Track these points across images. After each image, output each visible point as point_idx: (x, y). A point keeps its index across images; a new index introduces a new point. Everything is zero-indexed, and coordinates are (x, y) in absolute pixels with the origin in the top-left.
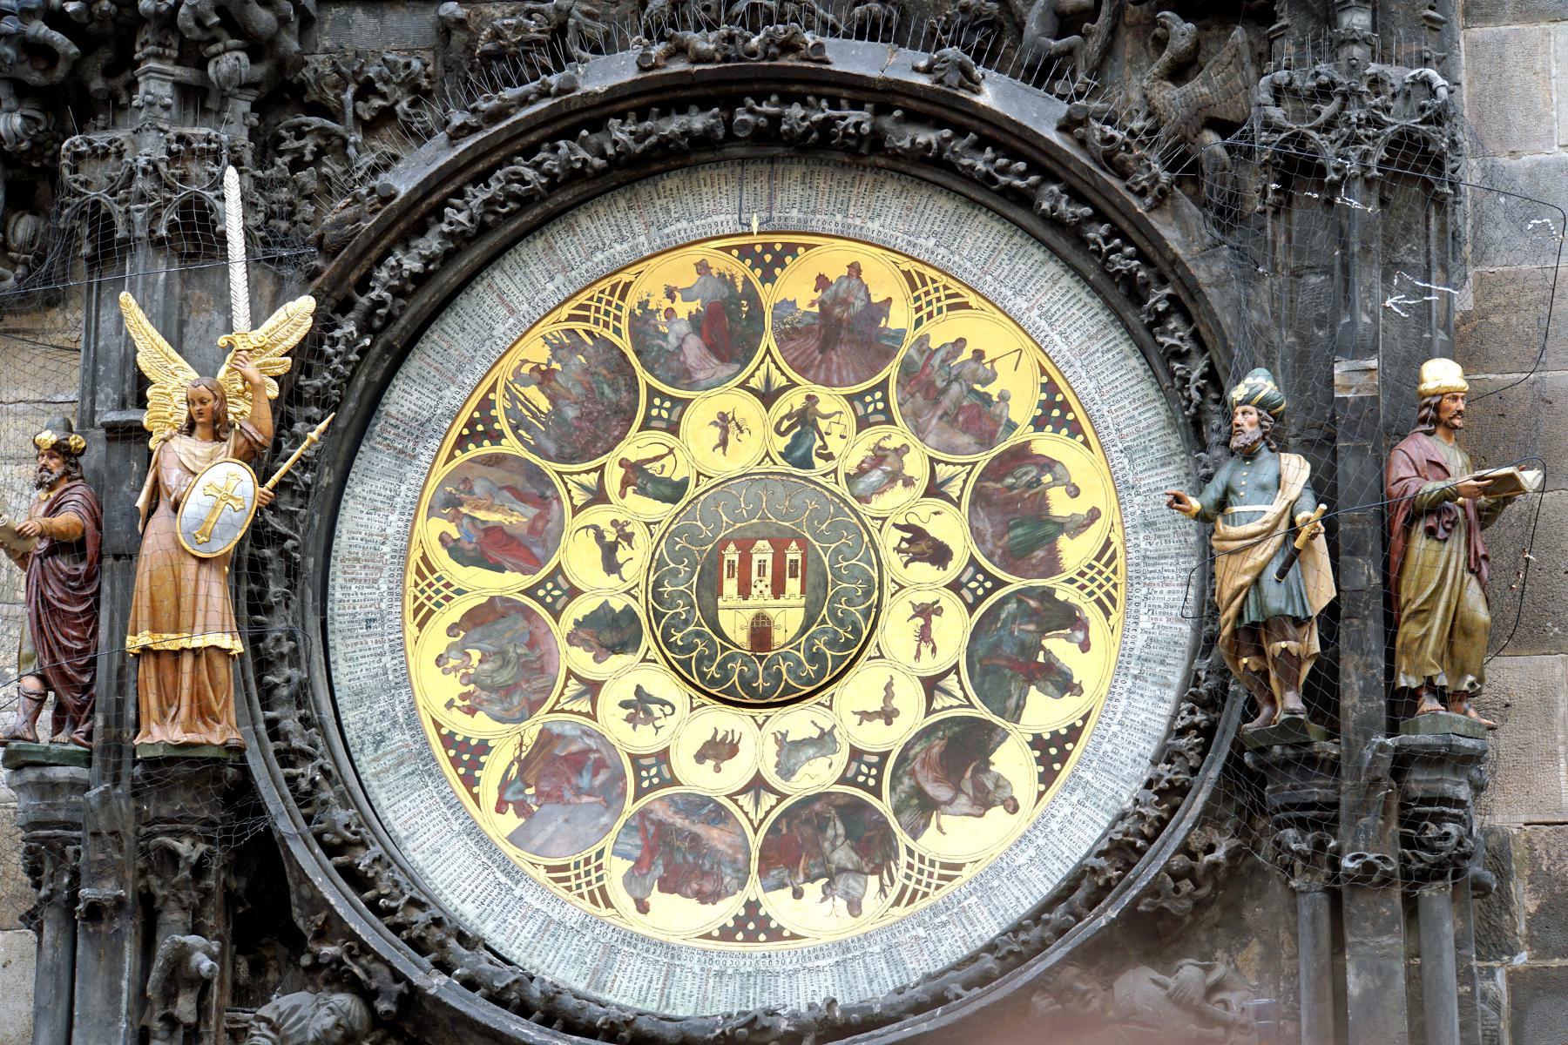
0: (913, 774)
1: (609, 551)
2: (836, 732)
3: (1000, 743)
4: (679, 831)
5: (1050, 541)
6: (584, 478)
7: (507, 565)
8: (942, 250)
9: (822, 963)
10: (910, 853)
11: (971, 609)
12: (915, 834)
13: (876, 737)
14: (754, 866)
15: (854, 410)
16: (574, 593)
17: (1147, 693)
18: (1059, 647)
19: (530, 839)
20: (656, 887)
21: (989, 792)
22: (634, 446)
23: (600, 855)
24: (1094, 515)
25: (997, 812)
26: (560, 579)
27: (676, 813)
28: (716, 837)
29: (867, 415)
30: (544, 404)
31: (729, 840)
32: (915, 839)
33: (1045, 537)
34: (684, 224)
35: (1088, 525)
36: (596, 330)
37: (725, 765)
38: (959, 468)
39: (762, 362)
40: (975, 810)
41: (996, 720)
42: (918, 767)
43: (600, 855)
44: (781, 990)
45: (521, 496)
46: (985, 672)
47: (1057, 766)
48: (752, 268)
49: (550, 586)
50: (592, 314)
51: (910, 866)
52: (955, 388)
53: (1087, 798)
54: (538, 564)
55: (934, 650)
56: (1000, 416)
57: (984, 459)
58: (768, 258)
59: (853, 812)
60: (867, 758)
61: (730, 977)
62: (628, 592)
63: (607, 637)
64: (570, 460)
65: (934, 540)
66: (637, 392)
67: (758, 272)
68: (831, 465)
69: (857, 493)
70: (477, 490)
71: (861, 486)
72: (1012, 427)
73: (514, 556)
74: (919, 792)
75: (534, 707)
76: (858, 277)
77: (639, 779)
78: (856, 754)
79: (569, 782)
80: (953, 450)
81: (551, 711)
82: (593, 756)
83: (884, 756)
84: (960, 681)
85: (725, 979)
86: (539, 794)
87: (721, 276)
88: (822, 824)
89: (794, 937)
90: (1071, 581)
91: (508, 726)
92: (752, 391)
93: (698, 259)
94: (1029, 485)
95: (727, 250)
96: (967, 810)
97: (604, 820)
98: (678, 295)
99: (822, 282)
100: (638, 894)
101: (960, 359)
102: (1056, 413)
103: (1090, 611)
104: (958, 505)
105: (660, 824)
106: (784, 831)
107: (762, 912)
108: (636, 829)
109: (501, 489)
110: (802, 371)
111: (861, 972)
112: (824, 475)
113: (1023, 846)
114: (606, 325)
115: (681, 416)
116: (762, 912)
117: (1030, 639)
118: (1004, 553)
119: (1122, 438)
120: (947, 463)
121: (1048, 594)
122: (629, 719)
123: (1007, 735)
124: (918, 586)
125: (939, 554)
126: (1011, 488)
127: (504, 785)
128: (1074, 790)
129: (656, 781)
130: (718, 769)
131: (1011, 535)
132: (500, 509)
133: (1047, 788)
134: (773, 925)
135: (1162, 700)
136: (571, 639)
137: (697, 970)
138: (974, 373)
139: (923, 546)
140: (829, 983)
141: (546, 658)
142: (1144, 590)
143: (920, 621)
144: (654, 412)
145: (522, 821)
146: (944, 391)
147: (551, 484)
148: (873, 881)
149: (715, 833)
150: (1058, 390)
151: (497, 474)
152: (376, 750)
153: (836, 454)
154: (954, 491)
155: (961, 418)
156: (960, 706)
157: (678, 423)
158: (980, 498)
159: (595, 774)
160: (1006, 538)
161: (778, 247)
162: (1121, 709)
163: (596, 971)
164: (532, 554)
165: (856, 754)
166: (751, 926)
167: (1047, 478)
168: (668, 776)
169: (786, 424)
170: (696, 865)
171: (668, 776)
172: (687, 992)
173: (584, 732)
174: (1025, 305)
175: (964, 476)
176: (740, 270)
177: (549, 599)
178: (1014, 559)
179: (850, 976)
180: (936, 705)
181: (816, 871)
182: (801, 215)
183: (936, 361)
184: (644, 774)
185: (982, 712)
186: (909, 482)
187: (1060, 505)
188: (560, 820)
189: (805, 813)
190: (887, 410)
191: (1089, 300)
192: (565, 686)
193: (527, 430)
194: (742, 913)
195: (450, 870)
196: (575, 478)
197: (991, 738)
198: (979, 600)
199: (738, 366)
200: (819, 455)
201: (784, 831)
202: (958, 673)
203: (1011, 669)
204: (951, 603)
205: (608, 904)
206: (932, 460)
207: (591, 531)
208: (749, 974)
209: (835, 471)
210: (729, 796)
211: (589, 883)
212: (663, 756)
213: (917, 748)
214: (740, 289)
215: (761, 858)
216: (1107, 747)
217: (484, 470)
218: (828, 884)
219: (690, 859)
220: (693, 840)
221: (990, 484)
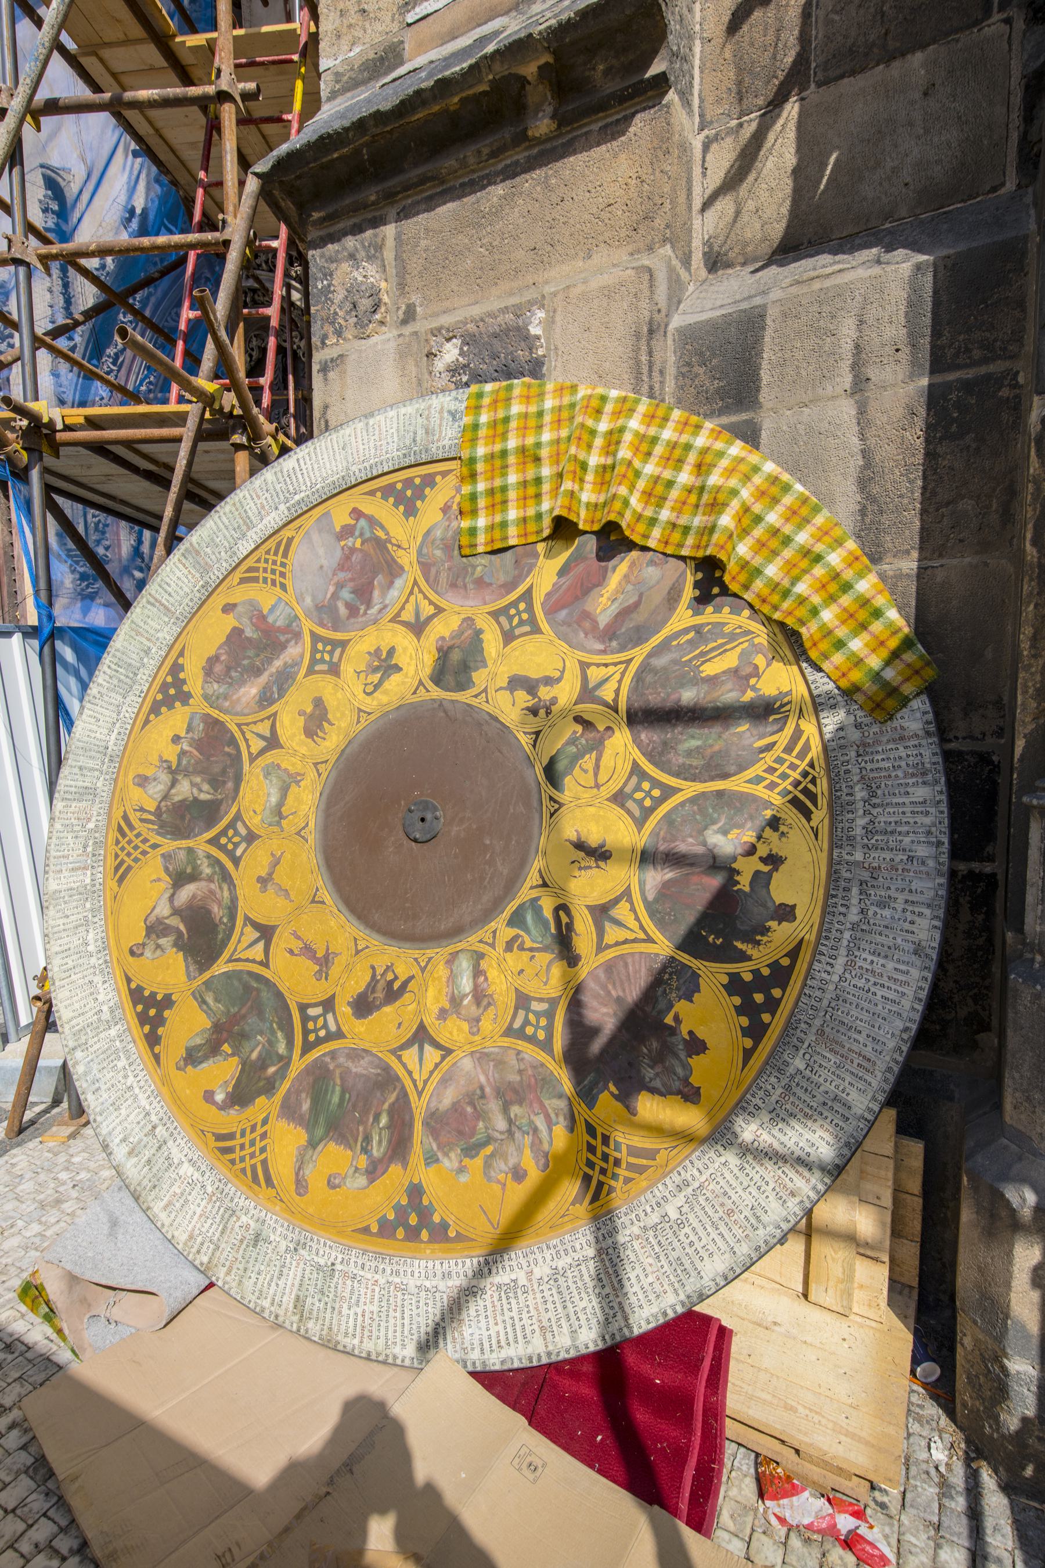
0: (210, 879)
1: (530, 686)
2: (276, 829)
3: (187, 967)
4: (270, 661)
5: (309, 1125)
6: (612, 685)
7: (563, 580)
8: (654, 1218)
9: (114, 736)
10: (155, 846)
11: (303, 1008)
12: (167, 857)
13: (255, 861)
14: (215, 713)
15: (541, 1000)
16: (508, 637)
17: (137, 1130)
18: (222, 1072)
19: (320, 531)
20: (237, 624)
21: (158, 937)
22: (622, 749)
23: (283, 587)
24: (301, 1185)
25: (140, 936)
26: (527, 628)
27: (285, 663)
28: (251, 691)
29: (528, 1010)
30: (709, 669)
31: (244, 700)
32: (163, 855)
33: (316, 1122)
34: (853, 916)
35: (297, 1174)
36: (769, 758)
37: (301, 721)
38: (425, 1076)
39: (642, 927)
40: (152, 918)
41: (207, 975)
42: (212, 886)
43: (283, 587)
44: (113, 695)
45: (625, 613)
46: (247, 988)
47: (140, 1008)
48: (756, 973)
49: (525, 616)
50: (791, 759)
51: (145, 841)
52: (501, 1124)
53: (99, 1020)
54: (551, 611)
55: (291, 952)
56: (446, 1155)
57: (419, 1107)
58: (759, 998)
59: (207, 813)
60: (243, 845)
61: (142, 659)
62: (485, 690)
63: (456, 656)
64: (638, 678)
65: (378, 1008)
66: (677, 775)
67: (748, 977)
68: (500, 946)
69: (461, 956)
70: (651, 569)
71: (465, 964)
72: (431, 1159)
73: (568, 589)
74: (193, 878)
75: (425, 567)
76: (679, 1092)
77: (327, 641)
78: (251, 838)
79: (352, 580)
80: (444, 1081)
81: (415, 583)
82: (363, 608)
83: (236, 861)
84: (254, 961)
85: (142, 654)
86: (353, 550)
87: (765, 931)
88: (216, 783)
89: (147, 722)
90: (265, 1122)
91: (419, 539)
92: (616, 901)
93: (799, 912)
94: (368, 1139)
95: (794, 954)
96: (157, 911)
97: (308, 600)
98: (766, 869)
99: (697, 1046)
100: (239, 609)
101: (527, 1152)
102: (413, 1220)
103: (233, 1120)
104: (393, 1052)
105: (283, 647)
106: (227, 749)
107: (178, 704)
108: (289, 625)
109: (641, 596)
110: (609, 967)
111: (91, 764)
112: (494, 932)
113: (99, 943)
114: (771, 770)
115: (629, 812)
116: (178, 704)
117: (247, 1046)
118: (328, 1070)
119: (345, 1274)
120: (437, 1065)
121: (269, 1088)
122: (378, 650)
123: (190, 978)
124: (348, 968)
125: (363, 1006)
126: (377, 1118)
127: (372, 521)
128: (112, 1012)
129: (318, 656)
130: (302, 713)
131: (338, 1089)
132: (620, 590)
133: (130, 989)
134: (164, 709)
135: (124, 1140)
136: (469, 621)
137: (160, 635)
138: (505, 1157)
139: (380, 995)
140: (98, 735)
141: (462, 591)
142: (209, 1189)
143: (320, 954)
144: (646, 786)
145: (338, 529)
146: (505, 1109)
147: (622, 648)
148: (151, 806)
149: (254, 691)
150: (432, 1239)
151: (657, 597)
152: (449, 412)
153: (508, 955)
154: (410, 1056)
155: (469, 1109)
156: (235, 950)
157: (622, 806)
158: (387, 1080)
159: (348, 605)
160: (338, 1081)
161: (766, 1017)
162: (141, 1096)
163: (197, 553)
164: (563, 607)
165: (251, 838)
166: (172, 691)
167: (363, 1162)
168: (317, 668)
169: (565, 919)
170: (239, 665)
171: (317, 668)
172: (149, 621)
173: (386, 607)
174: (537, 1272)
175: (416, 1076)
176: (761, 956)
177: (513, 611)
178: (318, 1078)
179: (93, 754)
180: (249, 929)
181: (184, 762)
182: (791, 1070)
183: (540, 1122)
184: (329, 648)
185: (221, 967)
186: (443, 1014)
187: (335, 1156)
188: (324, 562)
189: (231, 772)
190: (520, 1034)
191: (503, 1354)
192: (431, 603)
193: (689, 641)
194: (185, 688)
195: (325, 456)
196: (617, 676)
197: (196, 962)
198: (305, 1019)
199: (650, 897)
200: (516, 937)
201: (227, 749)
202: (261, 963)
203: (235, 1015)
204: (319, 991)
205: (243, 581)
206: (448, 1052)
207: (557, 674)
208: (136, 674)
209: (493, 946)
210: (275, 714)
211: (265, 570)
212: (334, 670)
213: (226, 894)
214: (739, 945)
215: (217, 722)
216: (120, 1064)
217: (667, 584)
218: (170, 767)
219: (245, 662)
220: (259, 670)
221: (392, 1098)
